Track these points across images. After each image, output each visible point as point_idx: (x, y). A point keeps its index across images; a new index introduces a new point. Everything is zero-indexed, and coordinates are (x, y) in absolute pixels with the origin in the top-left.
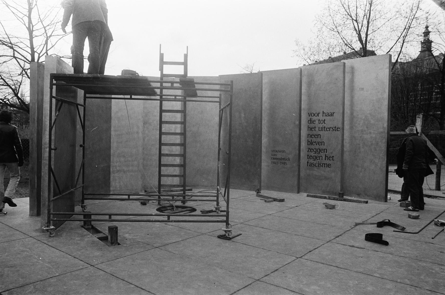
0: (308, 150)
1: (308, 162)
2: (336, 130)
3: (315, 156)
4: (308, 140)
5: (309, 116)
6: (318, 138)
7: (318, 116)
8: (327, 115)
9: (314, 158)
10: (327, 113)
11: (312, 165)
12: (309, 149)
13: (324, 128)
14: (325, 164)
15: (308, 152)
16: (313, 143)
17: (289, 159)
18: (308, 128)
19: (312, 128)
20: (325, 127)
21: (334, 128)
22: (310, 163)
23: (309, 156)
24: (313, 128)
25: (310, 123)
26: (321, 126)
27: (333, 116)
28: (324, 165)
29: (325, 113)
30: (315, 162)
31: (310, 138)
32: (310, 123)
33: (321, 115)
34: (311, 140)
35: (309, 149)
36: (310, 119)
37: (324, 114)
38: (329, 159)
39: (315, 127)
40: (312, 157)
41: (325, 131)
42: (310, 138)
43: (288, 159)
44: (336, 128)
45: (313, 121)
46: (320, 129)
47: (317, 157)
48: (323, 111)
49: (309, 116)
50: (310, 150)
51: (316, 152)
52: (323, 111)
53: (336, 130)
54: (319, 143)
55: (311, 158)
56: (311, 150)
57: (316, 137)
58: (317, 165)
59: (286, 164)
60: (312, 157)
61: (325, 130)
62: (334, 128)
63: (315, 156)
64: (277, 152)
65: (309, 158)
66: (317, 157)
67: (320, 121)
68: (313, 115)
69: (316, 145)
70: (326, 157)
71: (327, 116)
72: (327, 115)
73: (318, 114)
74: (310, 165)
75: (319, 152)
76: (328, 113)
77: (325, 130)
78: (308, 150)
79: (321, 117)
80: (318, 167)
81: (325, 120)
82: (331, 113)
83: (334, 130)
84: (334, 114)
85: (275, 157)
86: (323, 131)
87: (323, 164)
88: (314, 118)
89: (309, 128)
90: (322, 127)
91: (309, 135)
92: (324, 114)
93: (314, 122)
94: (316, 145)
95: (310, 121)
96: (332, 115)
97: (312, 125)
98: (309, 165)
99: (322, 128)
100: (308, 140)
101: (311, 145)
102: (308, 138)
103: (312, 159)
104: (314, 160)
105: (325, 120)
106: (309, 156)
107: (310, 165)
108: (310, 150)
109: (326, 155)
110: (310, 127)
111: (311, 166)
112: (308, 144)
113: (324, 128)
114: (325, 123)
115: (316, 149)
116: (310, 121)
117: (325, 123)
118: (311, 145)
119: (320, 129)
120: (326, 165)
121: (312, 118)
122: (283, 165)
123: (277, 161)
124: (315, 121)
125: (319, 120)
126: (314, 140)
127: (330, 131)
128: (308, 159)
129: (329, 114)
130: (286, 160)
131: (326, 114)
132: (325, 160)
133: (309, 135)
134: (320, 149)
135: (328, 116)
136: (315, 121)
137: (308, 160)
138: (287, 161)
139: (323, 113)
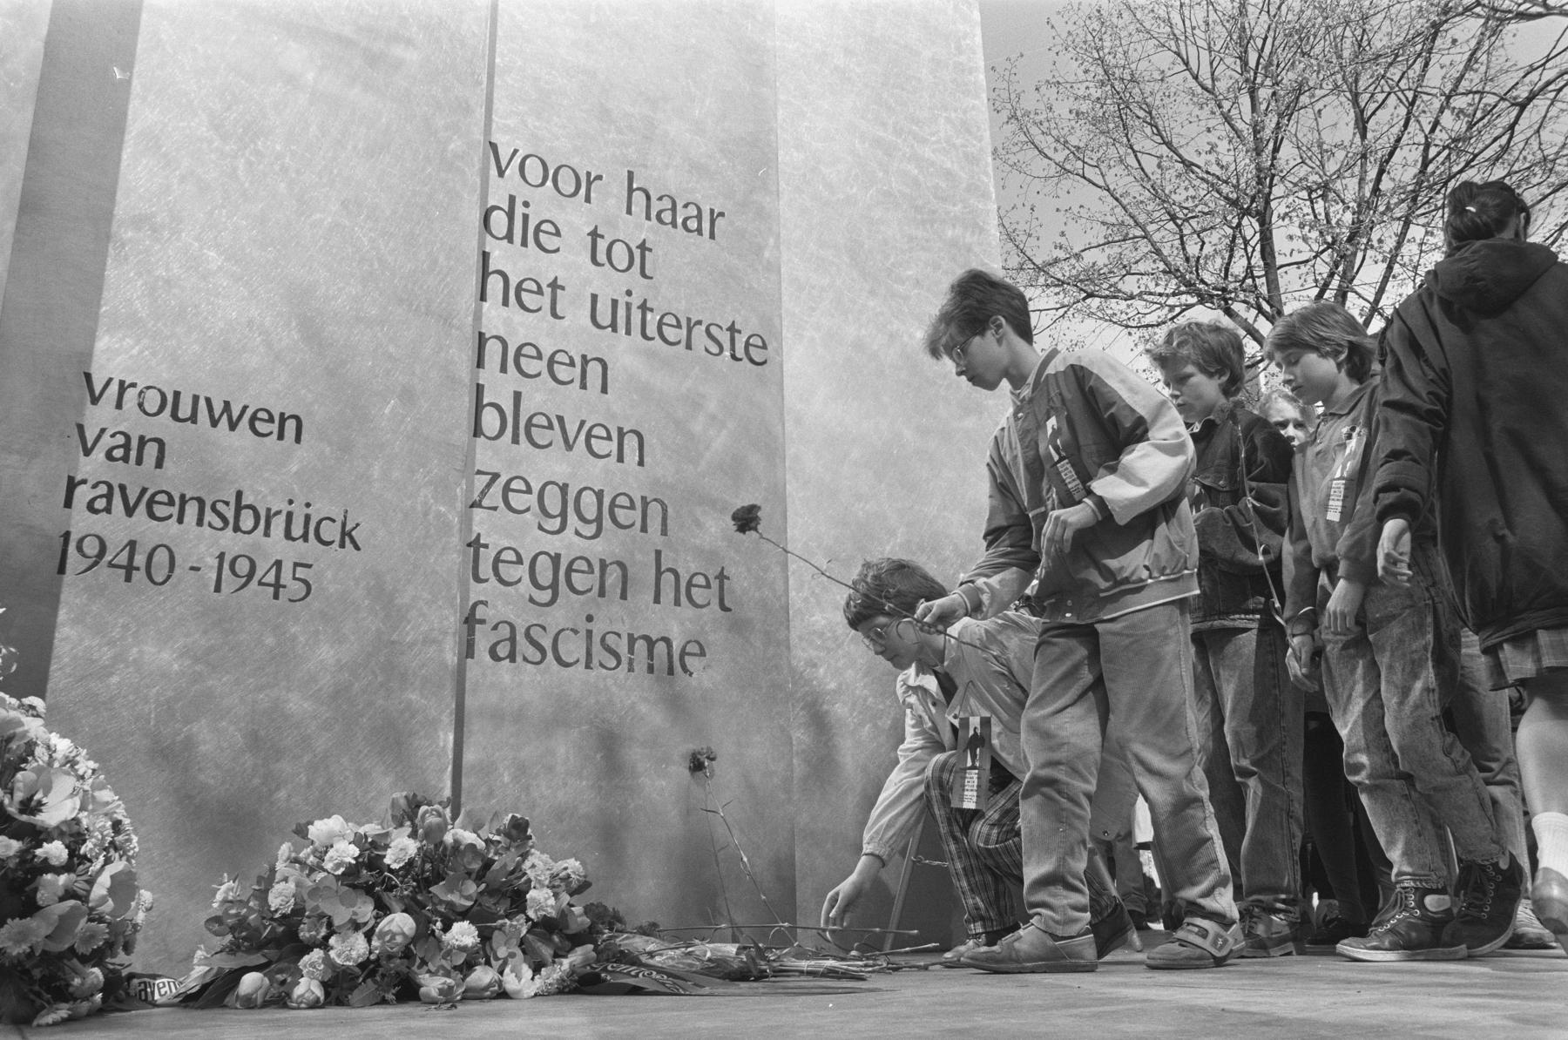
0: (483, 494)
1: (480, 612)
2: (740, 353)
3: (556, 559)
4: (479, 389)
5: (501, 173)
6: (583, 386)
7: (588, 200)
8: (667, 217)
9: (545, 577)
10: (667, 204)
11: (523, 645)
12: (496, 476)
13: (636, 316)
14: (651, 643)
16: (529, 424)
20: (644, 308)
22: (505, 631)
24: (540, 292)
25: (509, 237)
26: (609, 284)
27: (712, 236)
28: (641, 646)
30: (557, 617)
31: (504, 369)
34: (517, 396)
35: (496, 476)
36: (512, 199)
37: (639, 197)
38: (685, 592)
40: (520, 561)
41: (644, 335)
42: (504, 369)
43: (331, 532)
44: (740, 341)
46: (604, 318)
47: (570, 570)
48: (631, 174)
49: (501, 173)
50: (497, 488)
51: (563, 514)
53: (740, 353)
54: (589, 436)
56: (507, 488)
57: (563, 373)
58: (573, 648)
60: (520, 561)
61: (652, 330)
62: (724, 338)
63: (556, 559)
65: (486, 570)
66: (570, 570)
67: (602, 245)
68: (534, 171)
69: (569, 447)
70: (659, 573)
72: (667, 217)
73: (589, 183)
74: (503, 650)
75: (599, 519)
77: (652, 330)
78: (483, 494)
80: (588, 666)
84: (719, 222)
86: (628, 332)
87: (632, 640)
88: (542, 204)
90: (622, 300)
92: (639, 197)
94: (569, 446)
95: (511, 215)
101: (515, 440)
103: (526, 587)
104: (545, 596)
107: (503, 650)
108: (497, 488)
109: (658, 553)
111: (512, 657)
112: (477, 431)
113: (636, 316)
115: (564, 489)
116: (511, 215)
117: (643, 274)
118: (515, 440)
119: (604, 318)
120: (660, 648)
121: (524, 192)
124: (558, 233)
125: (595, 235)
126: (539, 397)
127: (689, 347)
128: (478, 579)
130: (312, 531)
131: (656, 206)
132: (657, 600)
133: (493, 348)
134: (599, 495)
136: (558, 233)
139: (631, 190)
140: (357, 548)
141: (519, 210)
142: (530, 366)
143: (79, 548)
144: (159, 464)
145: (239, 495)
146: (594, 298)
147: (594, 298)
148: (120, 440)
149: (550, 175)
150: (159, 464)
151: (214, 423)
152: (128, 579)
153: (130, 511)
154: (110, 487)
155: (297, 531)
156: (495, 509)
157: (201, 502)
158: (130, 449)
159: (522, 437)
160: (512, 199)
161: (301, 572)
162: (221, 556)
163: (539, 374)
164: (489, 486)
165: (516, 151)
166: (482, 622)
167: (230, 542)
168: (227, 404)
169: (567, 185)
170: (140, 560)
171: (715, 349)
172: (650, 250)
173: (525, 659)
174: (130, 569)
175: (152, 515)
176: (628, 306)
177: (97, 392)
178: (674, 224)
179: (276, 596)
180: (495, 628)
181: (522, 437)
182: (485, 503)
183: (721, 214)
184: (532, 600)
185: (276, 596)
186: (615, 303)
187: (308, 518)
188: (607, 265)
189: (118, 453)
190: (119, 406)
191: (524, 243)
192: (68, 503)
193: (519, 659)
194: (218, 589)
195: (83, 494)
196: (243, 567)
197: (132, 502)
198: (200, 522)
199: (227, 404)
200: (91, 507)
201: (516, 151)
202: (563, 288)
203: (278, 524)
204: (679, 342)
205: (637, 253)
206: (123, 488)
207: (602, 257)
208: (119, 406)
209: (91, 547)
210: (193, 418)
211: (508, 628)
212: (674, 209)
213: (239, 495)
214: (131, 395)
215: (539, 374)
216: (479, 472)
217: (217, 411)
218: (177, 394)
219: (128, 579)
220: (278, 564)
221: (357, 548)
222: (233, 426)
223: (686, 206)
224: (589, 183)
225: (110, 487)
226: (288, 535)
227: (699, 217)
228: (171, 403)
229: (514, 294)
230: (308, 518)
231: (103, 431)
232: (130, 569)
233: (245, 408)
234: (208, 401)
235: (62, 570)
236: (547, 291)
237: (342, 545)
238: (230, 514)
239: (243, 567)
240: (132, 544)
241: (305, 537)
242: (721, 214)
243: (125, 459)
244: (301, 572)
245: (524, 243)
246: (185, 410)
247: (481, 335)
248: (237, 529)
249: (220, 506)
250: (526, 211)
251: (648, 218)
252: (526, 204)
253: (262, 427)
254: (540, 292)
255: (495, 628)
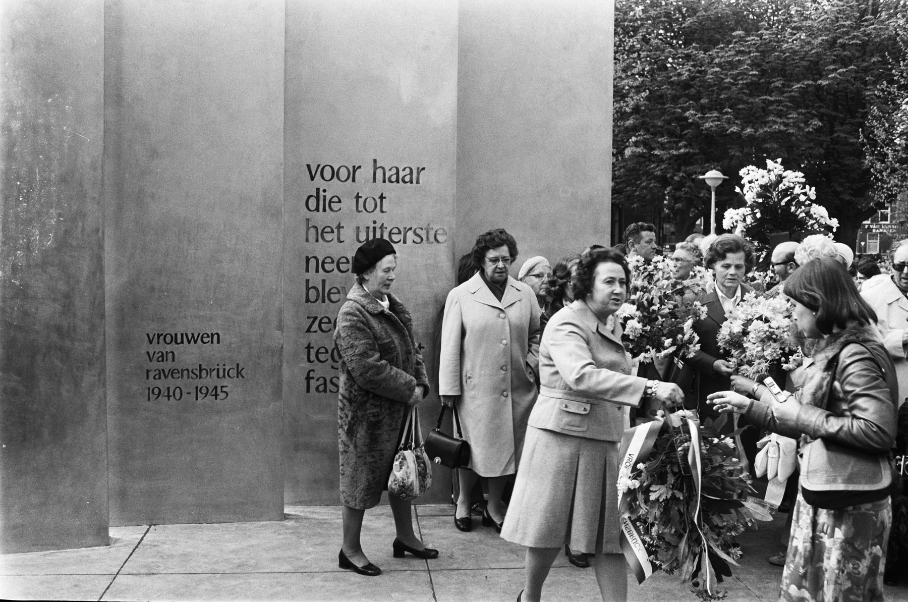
0: (310, 327)
1: (312, 374)
2: (432, 239)
4: (307, 281)
5: (312, 178)
7: (354, 180)
8: (394, 178)
10: (394, 171)
12: (315, 318)
15: (308, 331)
17: (239, 373)
18: (308, 229)
19: (329, 230)
20: (382, 227)
21: (423, 234)
22: (321, 381)
23: (313, 353)
24: (332, 232)
25: (317, 209)
27: (418, 182)
29: (383, 168)
31: (317, 271)
32: (317, 209)
33: (363, 175)
34: (324, 281)
36: (318, 189)
37: (379, 173)
39: (339, 227)
40: (327, 352)
42: (317, 271)
43: (233, 373)
45: (330, 202)
48: (375, 161)
49: (312, 178)
50: (317, 322)
52: (375, 161)
55: (322, 357)
56: (320, 323)
59: (222, 395)
64: (174, 339)
65: (313, 357)
67: (361, 201)
68: (328, 173)
71: (391, 182)
73: (354, 172)
76: (398, 169)
78: (310, 327)
79: (364, 184)
81: (382, 197)
82: (408, 171)
83: (422, 240)
85: (167, 366)
88: (333, 188)
89: (312, 231)
90: (372, 225)
91: (313, 263)
92: (379, 173)
93: (335, 206)
96: (413, 176)
97: (322, 219)
98: (313, 389)
99: (371, 229)
100: (307, 281)
101: (323, 301)
102: (307, 270)
105: (382, 197)
106: (313, 352)
107: (321, 388)
108: (317, 322)
110: (316, 227)
111: (325, 391)
114: (384, 210)
117: (382, 211)
118: (323, 301)
121: (322, 185)
122: (210, 398)
123: (179, 382)
124: (340, 201)
125: (358, 197)
127: (405, 242)
129: (401, 174)
133: (313, 263)
135: (397, 181)
136: (340, 201)
137: (309, 366)
138: (226, 382)
139: (375, 168)
140: (243, 377)
141: (322, 193)
142: (327, 267)
143: (153, 393)
144: (173, 360)
145: (200, 365)
146: (358, 228)
147: (358, 228)
148: (160, 354)
149: (335, 174)
150: (173, 360)
151: (189, 342)
152: (169, 399)
153: (166, 377)
154: (159, 371)
155: (221, 374)
156: (316, 332)
157: (188, 370)
158: (163, 357)
159: (327, 300)
160: (318, 189)
161: (224, 389)
162: (197, 388)
163: (333, 270)
164: (313, 322)
165: (319, 166)
166: (313, 378)
167: (199, 383)
168: (193, 335)
169: (343, 173)
170: (171, 394)
171: (418, 240)
172: (385, 198)
173: (331, 391)
174: (169, 396)
175: (173, 377)
176: (374, 228)
177: (151, 338)
178: (397, 181)
179: (216, 399)
180: (318, 380)
181: (327, 300)
182: (312, 330)
183: (423, 169)
184: (333, 367)
185: (216, 399)
186: (368, 228)
187: (224, 370)
188: (364, 211)
189: (160, 359)
190: (158, 343)
191: (324, 210)
192: (148, 378)
193: (328, 391)
194: (197, 399)
195: (151, 375)
196: (204, 391)
197: (166, 374)
198: (188, 378)
199: (193, 335)
200: (154, 378)
201: (319, 166)
202: (343, 227)
203: (215, 373)
204: (400, 241)
205: (378, 201)
206: (163, 370)
207: (361, 208)
208: (158, 343)
209: (156, 391)
210: (182, 342)
211: (322, 379)
212: (397, 173)
213: (200, 365)
214: (162, 338)
215: (333, 270)
216: (308, 318)
217: (190, 338)
218: (176, 335)
219: (169, 399)
220: (216, 388)
221: (243, 377)
222: (195, 342)
223: (404, 170)
224: (354, 172)
225: (159, 371)
226: (218, 376)
227: (411, 173)
228: (174, 339)
229: (321, 234)
230: (224, 370)
231: (155, 352)
232: (169, 396)
233: (199, 334)
234: (186, 334)
235: (149, 399)
236: (336, 231)
237: (238, 377)
238: (198, 373)
239: (204, 391)
240: (168, 388)
241: (224, 376)
242: (423, 169)
243: (163, 360)
244: (224, 389)
245: (324, 210)
246: (179, 341)
247: (307, 257)
248: (201, 377)
249: (195, 371)
250: (324, 194)
251: (384, 181)
252: (324, 191)
253: (205, 340)
254: (332, 232)
255: (318, 380)
